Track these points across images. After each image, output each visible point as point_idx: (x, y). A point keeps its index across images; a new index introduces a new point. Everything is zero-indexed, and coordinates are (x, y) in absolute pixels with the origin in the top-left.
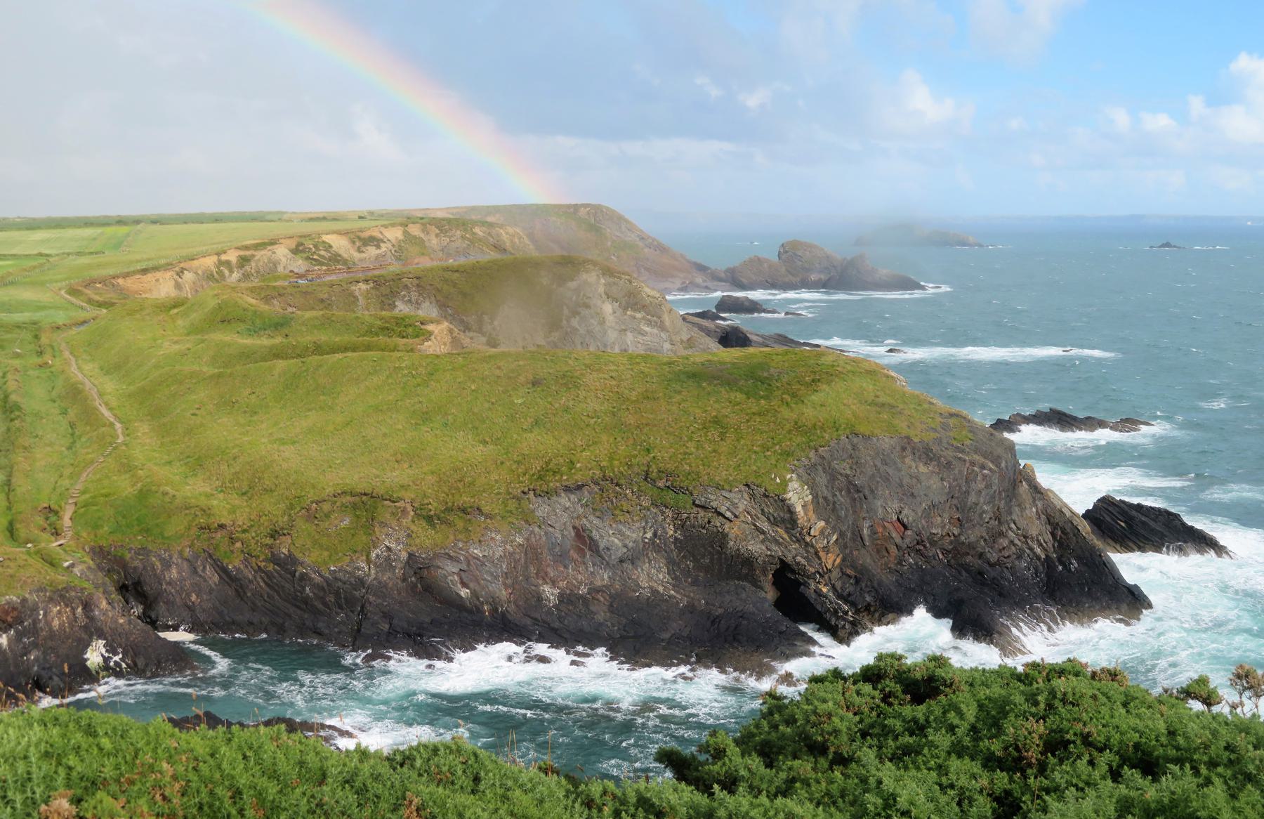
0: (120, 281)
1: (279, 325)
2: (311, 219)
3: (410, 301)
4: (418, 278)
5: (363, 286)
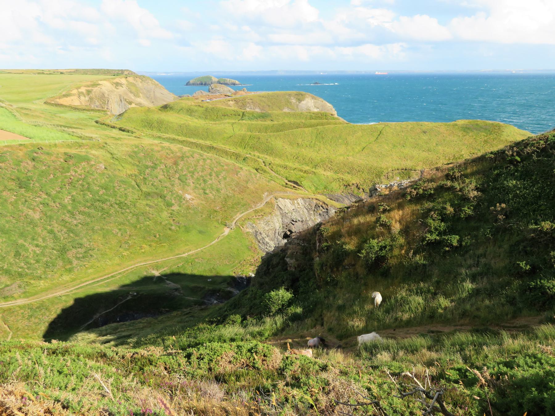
0: (58, 100)
2: (39, 73)
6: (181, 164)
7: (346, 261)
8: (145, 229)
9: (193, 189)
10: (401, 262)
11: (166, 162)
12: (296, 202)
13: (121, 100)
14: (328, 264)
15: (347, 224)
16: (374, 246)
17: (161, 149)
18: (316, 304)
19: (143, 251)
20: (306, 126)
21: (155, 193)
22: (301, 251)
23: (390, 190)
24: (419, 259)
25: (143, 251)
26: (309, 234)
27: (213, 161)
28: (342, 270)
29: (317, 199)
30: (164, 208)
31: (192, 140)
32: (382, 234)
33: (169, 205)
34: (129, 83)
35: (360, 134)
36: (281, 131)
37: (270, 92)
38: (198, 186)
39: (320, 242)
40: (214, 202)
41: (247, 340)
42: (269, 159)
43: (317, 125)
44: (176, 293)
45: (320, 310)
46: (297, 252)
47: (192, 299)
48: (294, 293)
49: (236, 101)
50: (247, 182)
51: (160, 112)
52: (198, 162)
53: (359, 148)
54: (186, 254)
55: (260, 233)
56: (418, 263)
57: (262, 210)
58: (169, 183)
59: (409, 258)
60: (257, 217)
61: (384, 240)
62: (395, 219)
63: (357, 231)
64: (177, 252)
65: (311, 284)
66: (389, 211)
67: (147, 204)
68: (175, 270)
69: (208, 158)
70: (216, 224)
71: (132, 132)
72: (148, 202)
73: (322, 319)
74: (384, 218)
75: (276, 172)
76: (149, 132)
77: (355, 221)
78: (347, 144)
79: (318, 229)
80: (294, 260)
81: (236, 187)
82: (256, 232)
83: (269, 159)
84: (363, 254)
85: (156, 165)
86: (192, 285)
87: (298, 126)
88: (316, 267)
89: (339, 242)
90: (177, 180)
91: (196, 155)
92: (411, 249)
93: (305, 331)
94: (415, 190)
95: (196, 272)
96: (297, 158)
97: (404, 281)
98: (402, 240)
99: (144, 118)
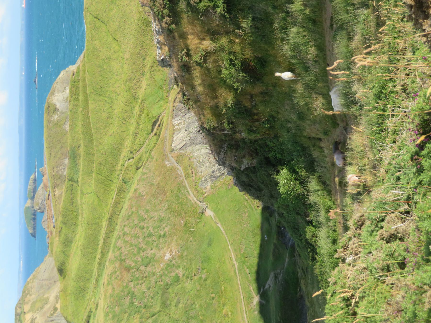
1: (74, 157)
3: (64, 169)
4: (53, 168)
5: (57, 193)
6: (129, 262)
7: (246, 105)
8: (205, 310)
9: (159, 250)
10: (250, 44)
11: (126, 281)
12: (177, 127)
13: (52, 321)
14: (249, 124)
15: (202, 98)
16: (230, 73)
17: (110, 286)
18: (296, 143)
19: (230, 313)
20: (86, 107)
21: (163, 295)
22: (234, 151)
23: (164, 44)
24: (246, 24)
25: (230, 313)
26: (213, 140)
27: (126, 223)
28: (257, 109)
29: (174, 102)
30: (180, 286)
31: (101, 242)
32: (215, 61)
33: (177, 280)
34: (32, 309)
35: (97, 42)
36: (91, 136)
37: (45, 145)
38: (155, 244)
39: (224, 130)
40: (174, 225)
41: (335, 226)
42: (125, 153)
43: (85, 92)
44: (280, 277)
45: (302, 138)
46: (235, 156)
47: (287, 260)
48: (283, 165)
49: (55, 186)
50: (152, 185)
51: (66, 278)
52: (126, 242)
53: (114, 45)
54: (235, 262)
55: (213, 172)
56: (251, 26)
57: (186, 169)
58: (152, 279)
59: (245, 34)
60: (194, 175)
61: (223, 60)
62: (199, 44)
63: (212, 89)
64: (232, 274)
65: (271, 144)
66: (188, 50)
67: (176, 306)
68: (252, 277)
69: (123, 230)
70: (200, 225)
71: (90, 312)
72: (173, 304)
73: (314, 138)
74: (196, 57)
75: (141, 145)
76: (90, 291)
77: (200, 89)
78: (109, 59)
79: (208, 130)
80: (244, 160)
81: (157, 197)
82: (211, 177)
83: (125, 153)
84: (238, 86)
85: (129, 293)
86: (271, 258)
87: (86, 116)
88: (253, 137)
89: (224, 110)
90: (147, 268)
91: (119, 244)
92: (234, 31)
93: (327, 159)
94: (164, 18)
95: (256, 252)
96: (124, 120)
97: (271, 44)
98: (224, 40)
99: (73, 297)
